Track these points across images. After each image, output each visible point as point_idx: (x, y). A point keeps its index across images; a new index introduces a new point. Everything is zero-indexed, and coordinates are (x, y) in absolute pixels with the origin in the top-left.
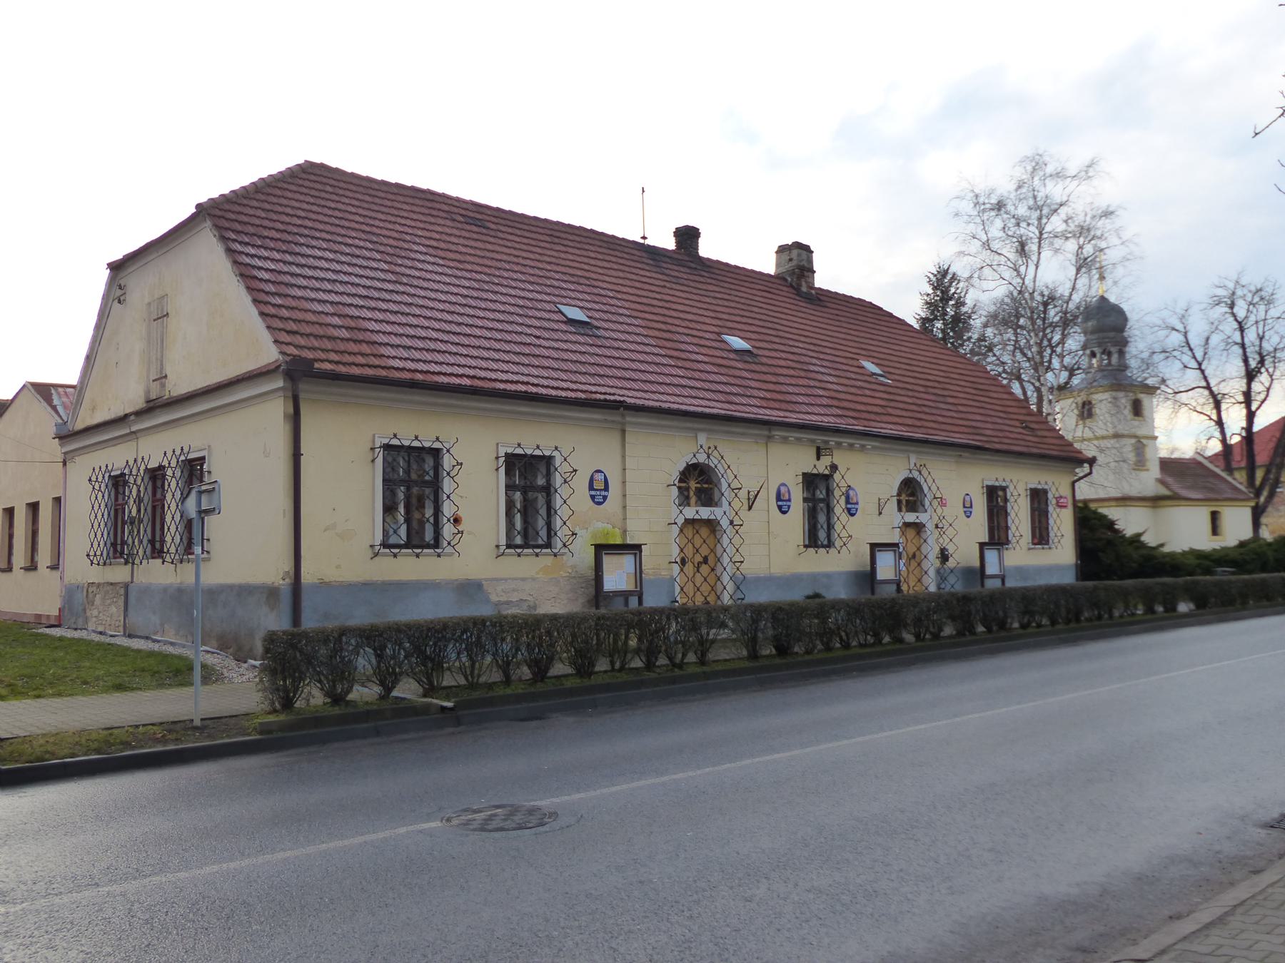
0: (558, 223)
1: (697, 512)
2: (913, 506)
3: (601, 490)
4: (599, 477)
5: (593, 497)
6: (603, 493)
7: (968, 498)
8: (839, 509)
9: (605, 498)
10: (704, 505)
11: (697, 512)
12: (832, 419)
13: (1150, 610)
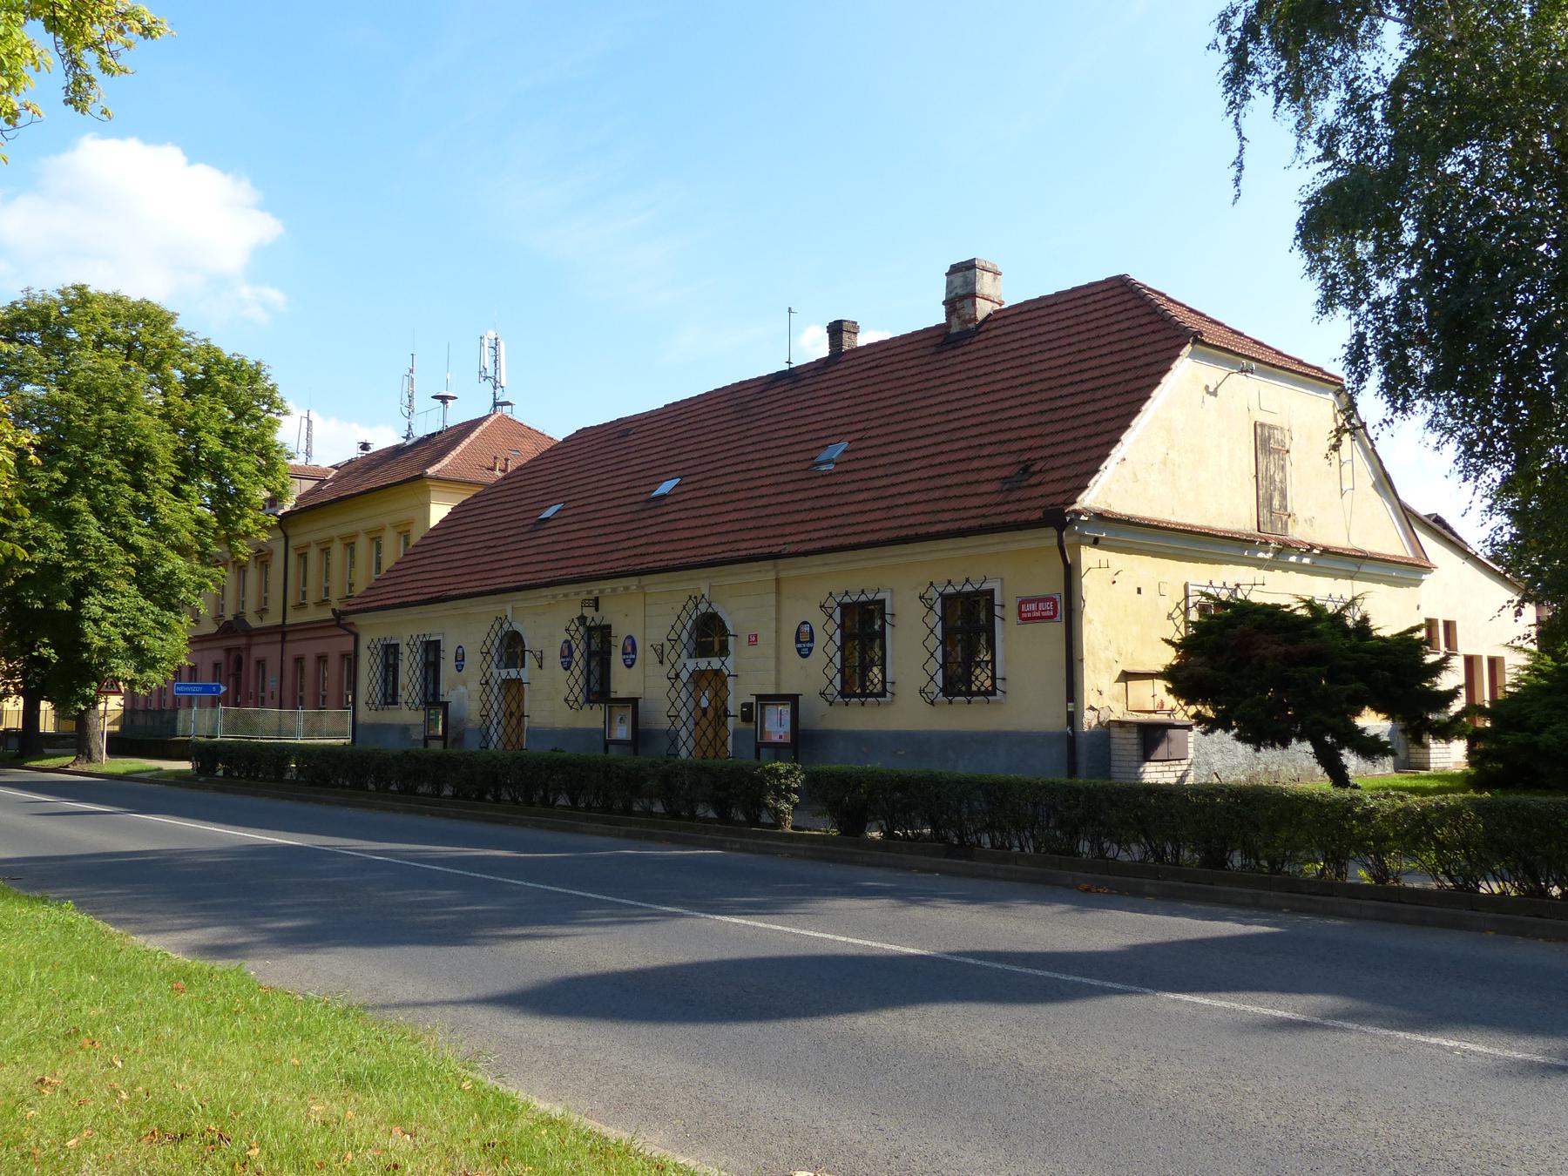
0: (1074, 290)
1: (709, 664)
2: (702, 650)
3: (807, 642)
4: (806, 628)
5: (799, 650)
6: (809, 645)
7: (460, 651)
8: (617, 658)
9: (810, 649)
10: (700, 657)
11: (709, 664)
12: (622, 563)
13: (724, 817)
